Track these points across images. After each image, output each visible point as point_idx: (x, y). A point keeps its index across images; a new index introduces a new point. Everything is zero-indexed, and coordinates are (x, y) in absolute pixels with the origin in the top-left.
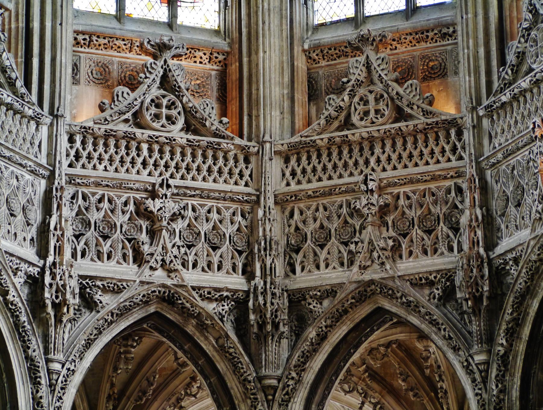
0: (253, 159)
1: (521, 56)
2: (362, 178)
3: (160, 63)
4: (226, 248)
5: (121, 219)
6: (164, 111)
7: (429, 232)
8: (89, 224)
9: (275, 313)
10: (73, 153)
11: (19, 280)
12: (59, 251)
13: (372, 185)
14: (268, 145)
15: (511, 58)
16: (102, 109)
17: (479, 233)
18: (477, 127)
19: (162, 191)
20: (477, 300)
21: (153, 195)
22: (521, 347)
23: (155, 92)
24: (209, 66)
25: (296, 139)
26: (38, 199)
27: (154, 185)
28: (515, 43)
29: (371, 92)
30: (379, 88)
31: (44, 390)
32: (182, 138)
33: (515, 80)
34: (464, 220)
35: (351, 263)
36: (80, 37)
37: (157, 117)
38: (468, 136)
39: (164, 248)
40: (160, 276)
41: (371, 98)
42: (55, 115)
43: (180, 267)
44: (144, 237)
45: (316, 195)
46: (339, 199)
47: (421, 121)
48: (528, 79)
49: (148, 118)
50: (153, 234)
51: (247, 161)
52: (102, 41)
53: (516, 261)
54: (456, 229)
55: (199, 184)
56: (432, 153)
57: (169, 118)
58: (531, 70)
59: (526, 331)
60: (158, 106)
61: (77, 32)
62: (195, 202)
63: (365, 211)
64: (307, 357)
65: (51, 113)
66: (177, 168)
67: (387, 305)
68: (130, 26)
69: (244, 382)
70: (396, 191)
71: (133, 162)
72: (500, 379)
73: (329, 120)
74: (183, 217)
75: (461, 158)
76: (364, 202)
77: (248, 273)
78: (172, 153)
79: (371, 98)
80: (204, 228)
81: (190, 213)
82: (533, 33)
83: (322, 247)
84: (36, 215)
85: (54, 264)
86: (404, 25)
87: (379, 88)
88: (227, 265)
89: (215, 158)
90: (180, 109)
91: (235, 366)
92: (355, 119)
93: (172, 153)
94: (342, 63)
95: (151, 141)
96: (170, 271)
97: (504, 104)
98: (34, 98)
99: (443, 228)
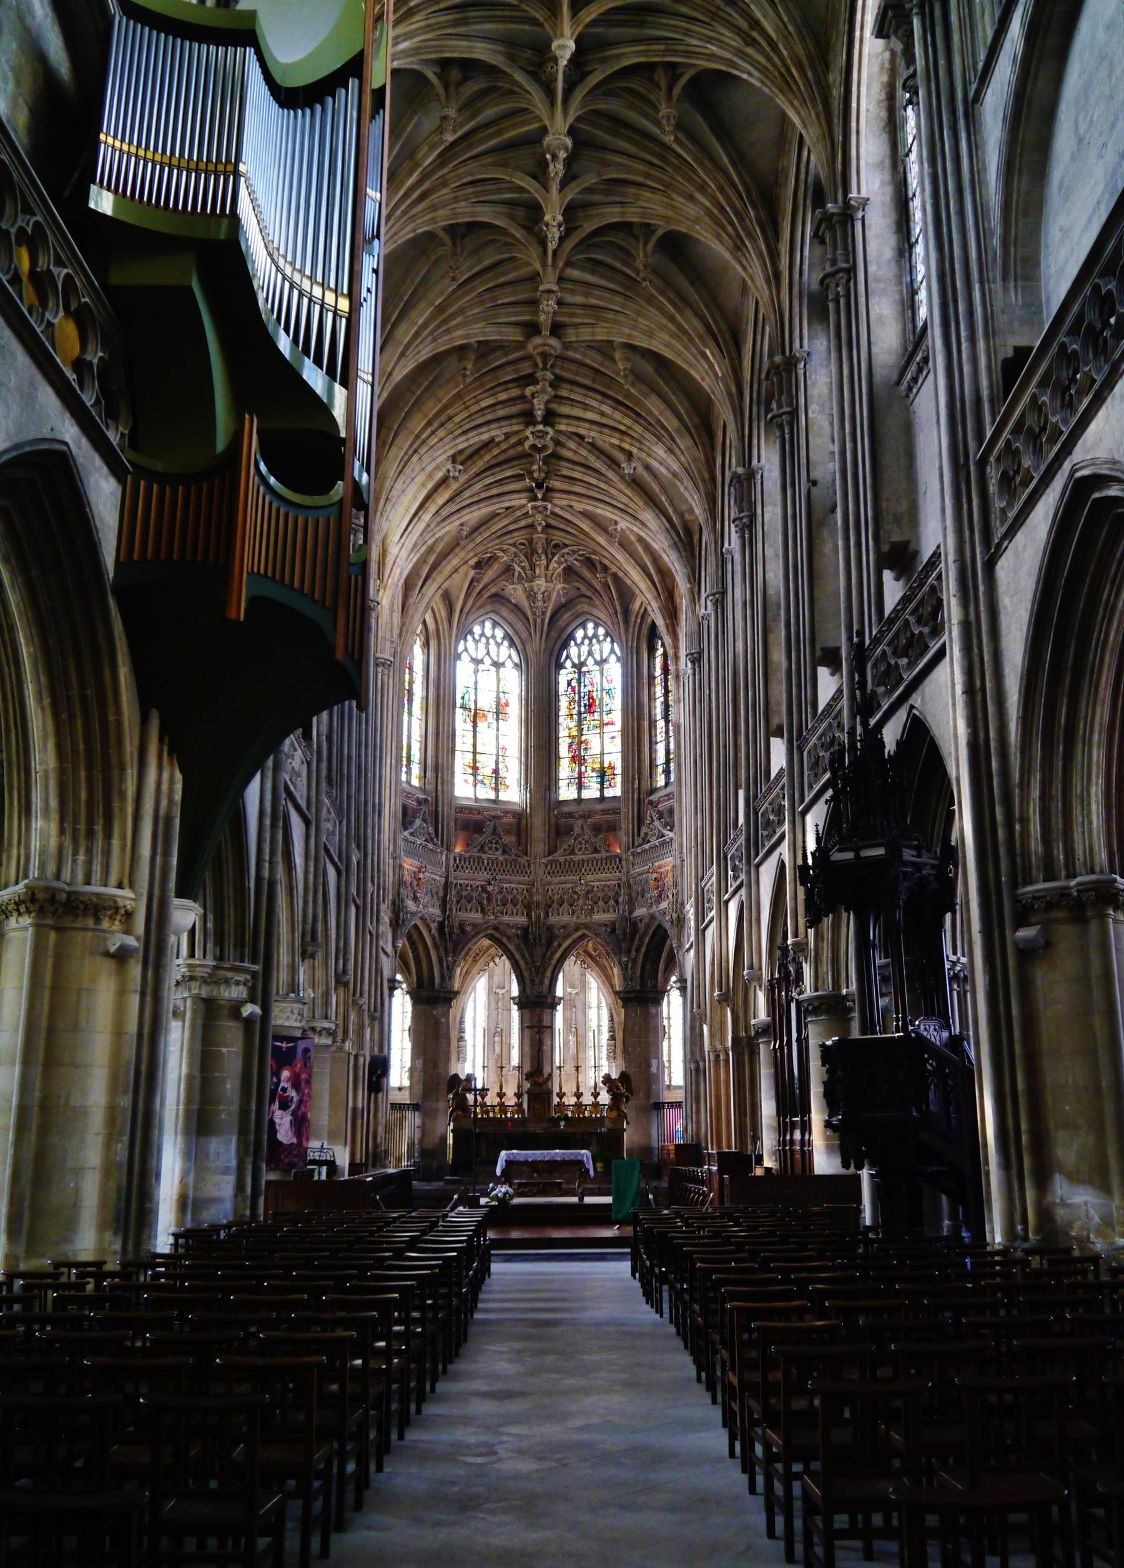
0: (532, 867)
1: (646, 834)
4: (519, 905)
7: (606, 903)
9: (540, 935)
12: (451, 910)
15: (642, 834)
16: (468, 845)
20: (625, 934)
21: (490, 884)
22: (641, 956)
26: (441, 888)
30: (586, 837)
31: (445, 969)
34: (620, 900)
38: (624, 863)
44: (485, 901)
45: (559, 883)
46: (568, 886)
47: (604, 854)
51: (529, 866)
54: (617, 902)
55: (508, 877)
59: (643, 950)
64: (553, 954)
67: (587, 932)
69: (527, 963)
72: (633, 967)
73: (565, 850)
77: (529, 916)
80: (510, 898)
84: (441, 894)
86: (599, 807)
87: (586, 837)
88: (520, 912)
91: (523, 957)
94: (571, 821)
95: (488, 859)
99: (612, 902)
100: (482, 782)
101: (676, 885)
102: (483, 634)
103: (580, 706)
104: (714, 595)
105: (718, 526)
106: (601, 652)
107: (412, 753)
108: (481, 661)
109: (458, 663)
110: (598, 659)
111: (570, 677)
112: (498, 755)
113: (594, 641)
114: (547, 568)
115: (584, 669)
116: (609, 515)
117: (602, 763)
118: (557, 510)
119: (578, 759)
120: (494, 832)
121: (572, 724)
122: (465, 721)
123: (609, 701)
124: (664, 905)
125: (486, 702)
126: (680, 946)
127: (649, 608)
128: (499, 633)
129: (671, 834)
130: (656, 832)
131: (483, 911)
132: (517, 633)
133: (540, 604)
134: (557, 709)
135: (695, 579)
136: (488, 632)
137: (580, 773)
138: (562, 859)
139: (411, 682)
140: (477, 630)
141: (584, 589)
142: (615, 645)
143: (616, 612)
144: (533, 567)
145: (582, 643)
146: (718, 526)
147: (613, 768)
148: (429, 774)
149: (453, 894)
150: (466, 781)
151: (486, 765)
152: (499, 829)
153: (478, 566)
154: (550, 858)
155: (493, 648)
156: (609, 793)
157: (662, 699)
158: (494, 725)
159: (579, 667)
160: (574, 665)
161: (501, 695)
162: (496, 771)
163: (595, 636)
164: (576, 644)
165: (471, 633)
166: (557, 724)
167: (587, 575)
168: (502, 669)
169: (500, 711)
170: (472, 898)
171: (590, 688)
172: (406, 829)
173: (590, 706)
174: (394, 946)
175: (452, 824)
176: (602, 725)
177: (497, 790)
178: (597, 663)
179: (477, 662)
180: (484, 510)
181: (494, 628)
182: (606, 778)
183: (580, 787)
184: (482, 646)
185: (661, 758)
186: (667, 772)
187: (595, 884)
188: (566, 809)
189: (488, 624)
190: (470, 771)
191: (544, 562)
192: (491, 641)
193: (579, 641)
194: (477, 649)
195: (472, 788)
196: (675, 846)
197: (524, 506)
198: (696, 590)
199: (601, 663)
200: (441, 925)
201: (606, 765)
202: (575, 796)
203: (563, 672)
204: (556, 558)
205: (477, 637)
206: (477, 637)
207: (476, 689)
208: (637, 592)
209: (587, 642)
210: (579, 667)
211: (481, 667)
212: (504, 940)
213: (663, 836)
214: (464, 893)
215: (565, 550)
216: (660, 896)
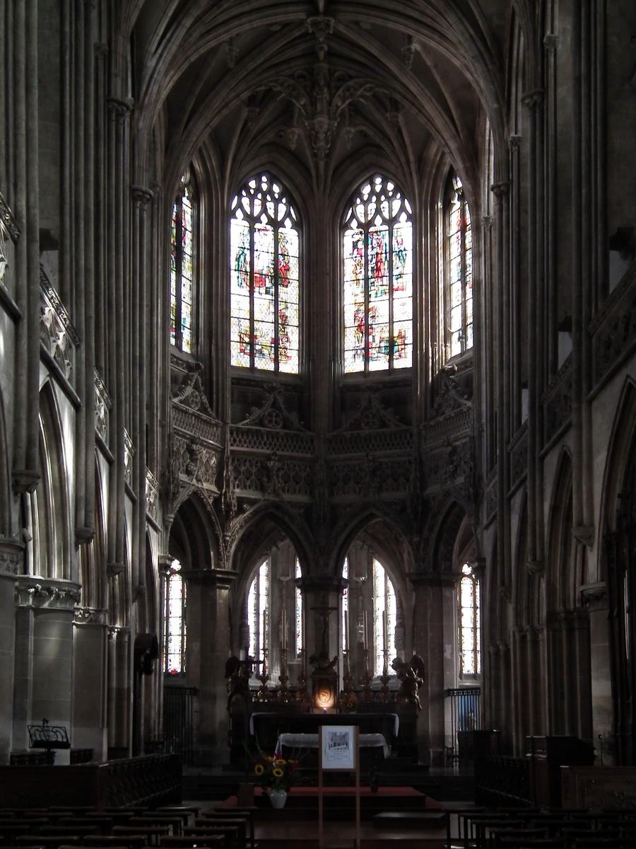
2: (365, 454)
3: (272, 396)
5: (254, 470)
6: (274, 419)
8: (240, 472)
10: (232, 439)
11: (211, 501)
12: (228, 486)
13: (370, 458)
14: (322, 436)
15: (436, 406)
17: (418, 484)
18: (419, 433)
19: (273, 457)
22: (434, 536)
23: (270, 410)
24: (294, 393)
25: (335, 433)
27: (269, 455)
28: (438, 398)
29: (371, 413)
32: (282, 432)
33: (435, 417)
34: (412, 477)
35: (360, 492)
36: (234, 381)
37: (270, 421)
39: (274, 483)
40: (272, 498)
41: (371, 416)
42: (225, 424)
43: (281, 492)
44: (265, 479)
48: (443, 417)
49: (266, 422)
50: (269, 480)
52: (244, 382)
53: (434, 499)
54: (408, 480)
56: (398, 444)
57: (276, 422)
58: (444, 413)
59: (436, 529)
60: (271, 416)
61: (233, 379)
62: (289, 462)
63: (367, 469)
65: (222, 421)
66: (280, 446)
68: (257, 375)
70: (381, 460)
71: (260, 444)
74: (283, 469)
75: (411, 447)
76: (367, 465)
77: (312, 494)
78: (278, 439)
79: (371, 416)
80: (292, 474)
81: (286, 467)
82: (446, 397)
83: (346, 484)
85: (226, 492)
86: (387, 378)
89: (297, 441)
90: (281, 417)
92: (363, 425)
93: (278, 439)
96: (277, 495)
97: (431, 426)
98: (214, 415)
100: (261, 352)
101: (473, 457)
102: (258, 189)
103: (366, 270)
104: (531, 96)
105: (538, 11)
106: (390, 210)
107: (183, 316)
108: (258, 220)
109: (233, 221)
110: (386, 215)
111: (357, 237)
112: (276, 322)
113: (383, 198)
114: (330, 103)
115: (372, 229)
116: (402, 29)
117: (391, 331)
118: (341, 28)
119: (365, 328)
120: (274, 405)
121: (359, 289)
122: (240, 285)
123: (399, 265)
124: (460, 480)
125: (263, 263)
126: (478, 522)
127: (446, 150)
128: (276, 189)
129: (469, 404)
130: (452, 402)
131: (262, 488)
132: (297, 187)
133: (322, 144)
134: (342, 275)
135: (504, 99)
136: (264, 187)
137: (367, 343)
138: (348, 434)
139: (180, 238)
140: (252, 184)
141: (371, 133)
142: (406, 202)
143: (408, 161)
144: (313, 103)
145: (369, 200)
146: (538, 11)
147: (404, 337)
148: (202, 339)
149: (229, 472)
150: (242, 351)
151: (265, 332)
152: (280, 400)
153: (251, 101)
154: (335, 433)
155: (270, 205)
156: (398, 364)
157: (459, 259)
158: (273, 290)
159: (366, 227)
160: (360, 225)
161: (281, 258)
162: (276, 341)
163: (384, 191)
164: (362, 200)
165: (247, 189)
166: (342, 291)
167: (378, 116)
168: (281, 230)
169: (278, 277)
170: (251, 474)
171: (379, 252)
172: (176, 395)
173: (378, 269)
174: (164, 521)
175: (228, 395)
176: (391, 290)
177: (276, 361)
178: (385, 222)
179: (252, 220)
180: (259, 22)
181: (270, 183)
182: (396, 348)
183: (367, 358)
184: (257, 202)
185: (456, 324)
186: (463, 338)
187: (383, 460)
188: (351, 381)
189: (264, 179)
190: (247, 340)
191: (326, 95)
192: (269, 198)
193: (366, 198)
194: (252, 205)
195: (247, 358)
196: (473, 415)
197: (302, 23)
198: (504, 110)
199: (391, 222)
200: (217, 501)
201: (396, 334)
202: (362, 369)
203: (348, 233)
204: (340, 92)
205: (252, 192)
206: (252, 192)
207: (252, 250)
208: (433, 131)
209: (374, 199)
210: (366, 227)
211: (257, 226)
212: (286, 519)
213: (459, 406)
214: (243, 469)
215: (351, 83)
216: (455, 471)
